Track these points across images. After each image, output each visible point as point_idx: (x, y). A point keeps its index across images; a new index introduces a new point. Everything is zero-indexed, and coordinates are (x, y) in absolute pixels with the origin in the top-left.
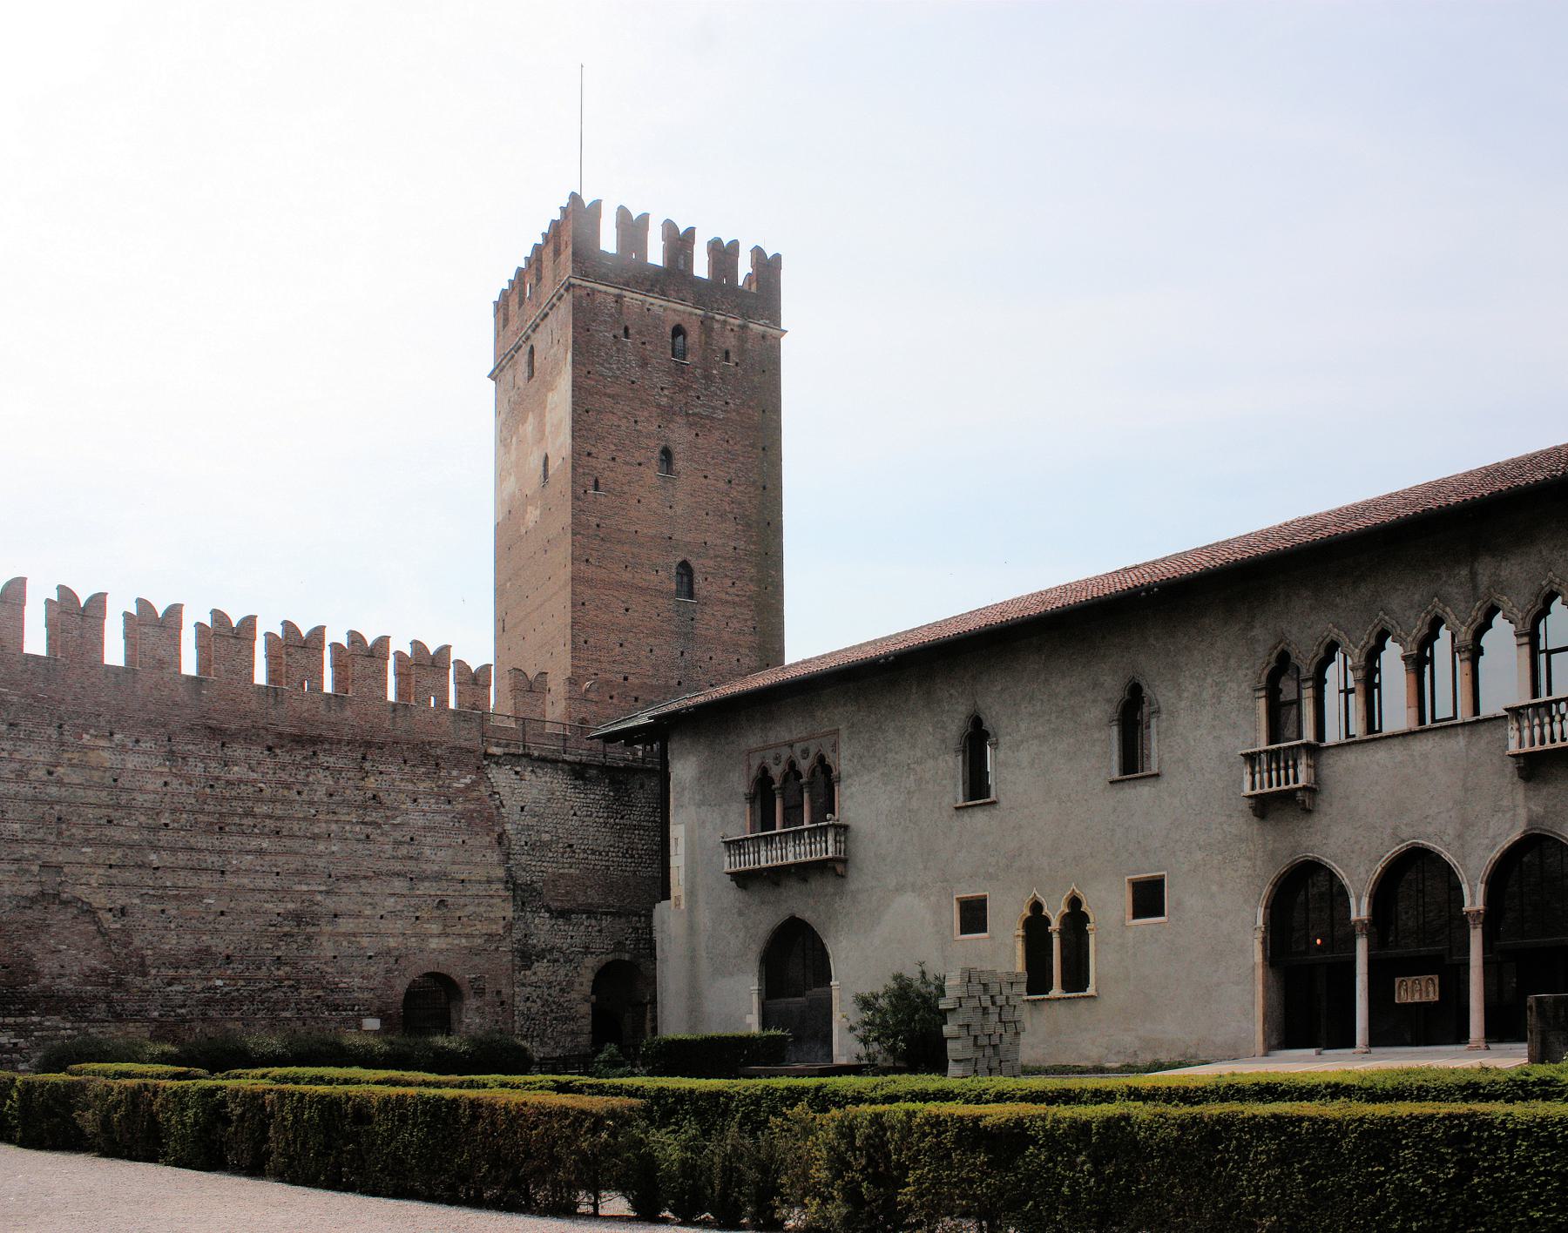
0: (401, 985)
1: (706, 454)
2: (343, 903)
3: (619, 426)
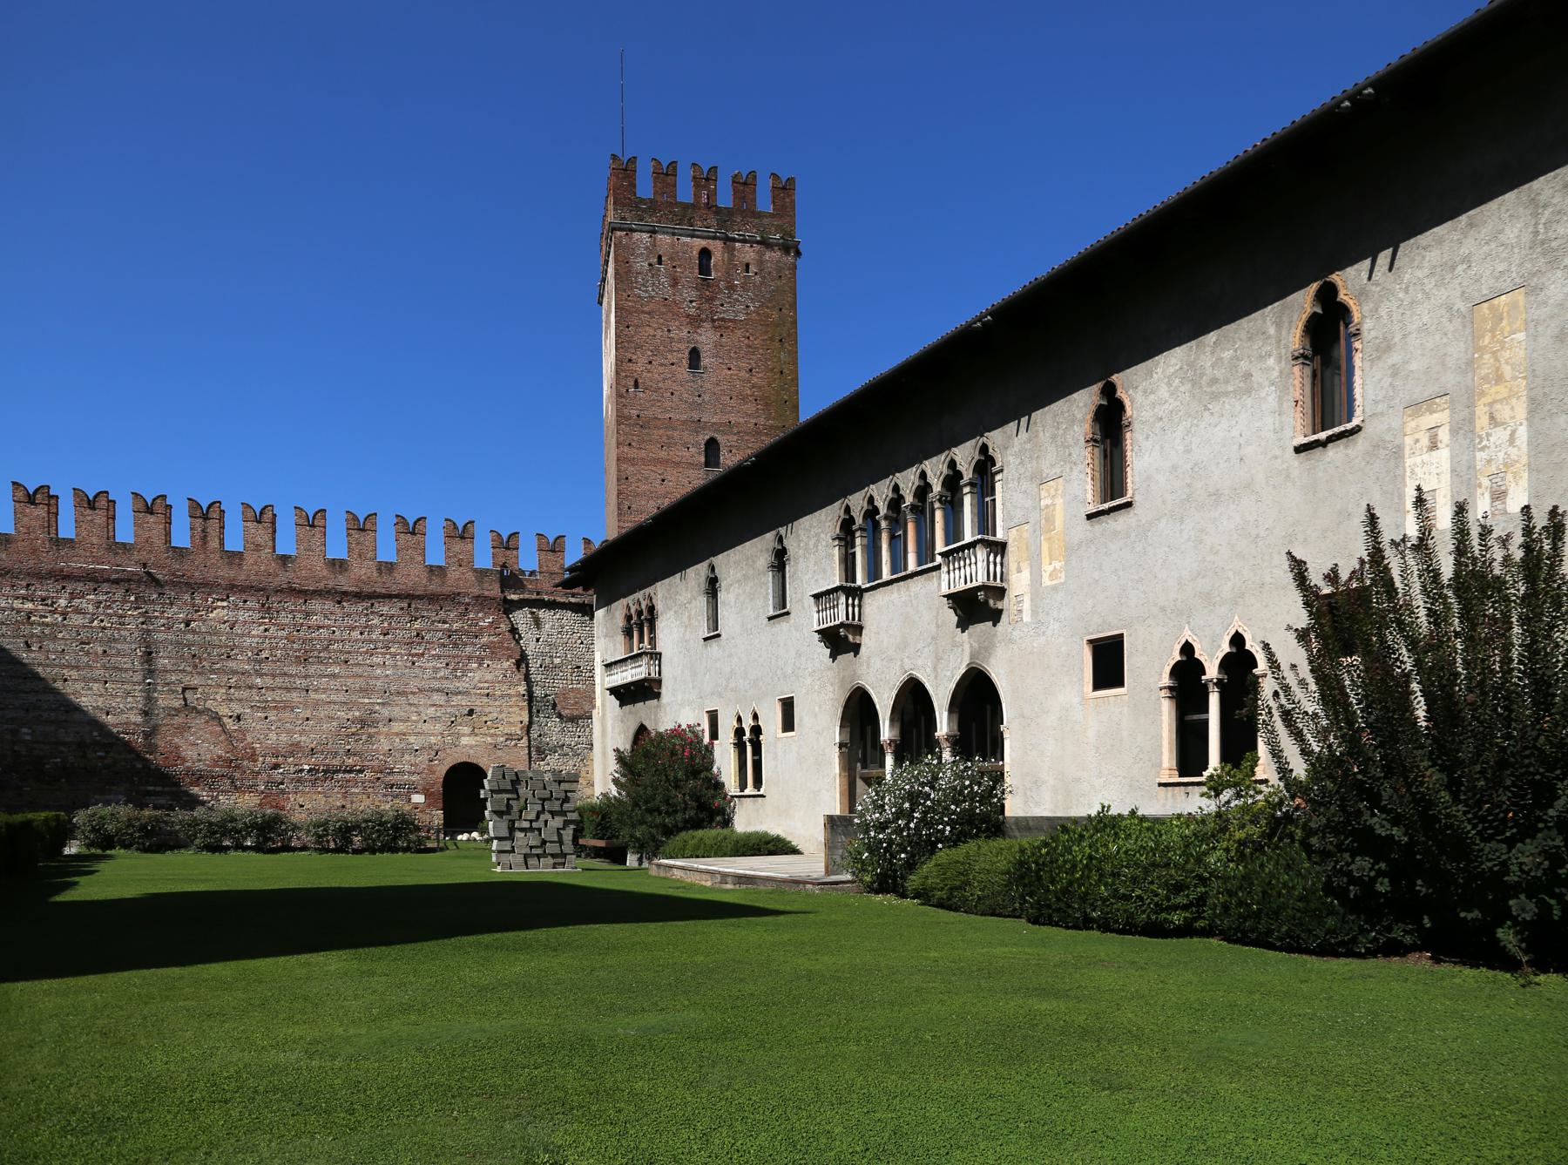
2: (396, 712)
3: (655, 336)
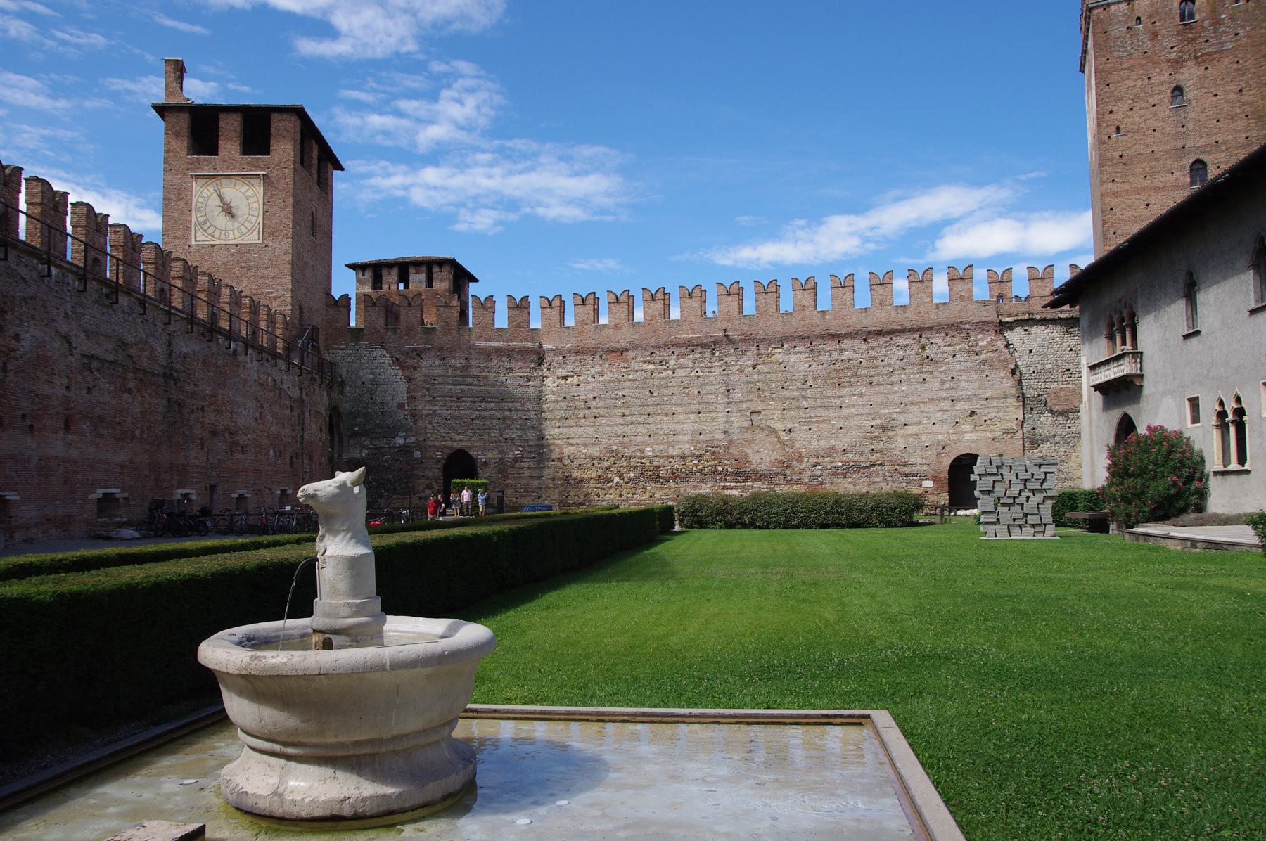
0: (947, 462)
1: (1215, 80)
3: (1135, 86)
